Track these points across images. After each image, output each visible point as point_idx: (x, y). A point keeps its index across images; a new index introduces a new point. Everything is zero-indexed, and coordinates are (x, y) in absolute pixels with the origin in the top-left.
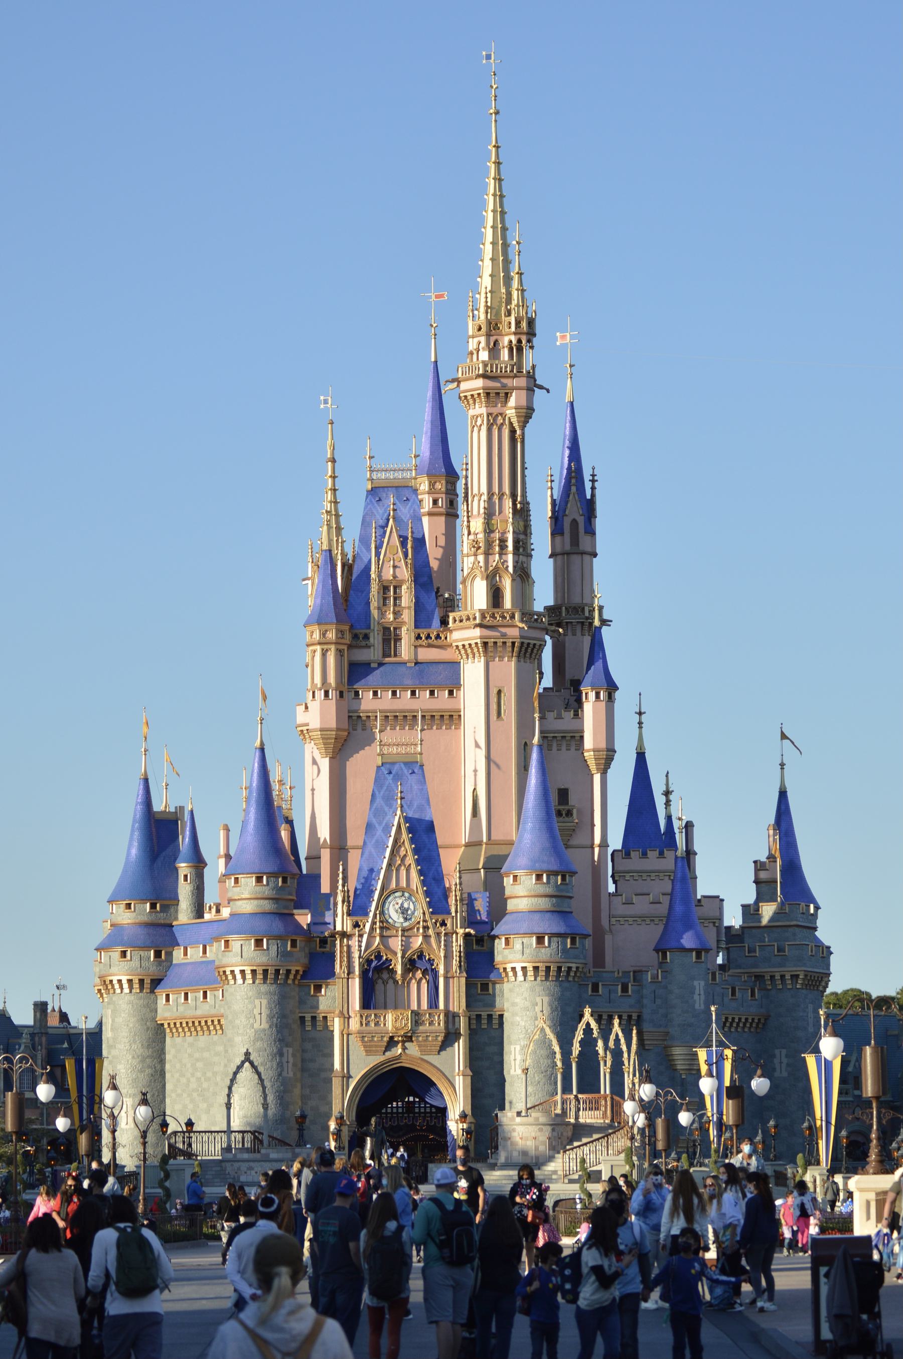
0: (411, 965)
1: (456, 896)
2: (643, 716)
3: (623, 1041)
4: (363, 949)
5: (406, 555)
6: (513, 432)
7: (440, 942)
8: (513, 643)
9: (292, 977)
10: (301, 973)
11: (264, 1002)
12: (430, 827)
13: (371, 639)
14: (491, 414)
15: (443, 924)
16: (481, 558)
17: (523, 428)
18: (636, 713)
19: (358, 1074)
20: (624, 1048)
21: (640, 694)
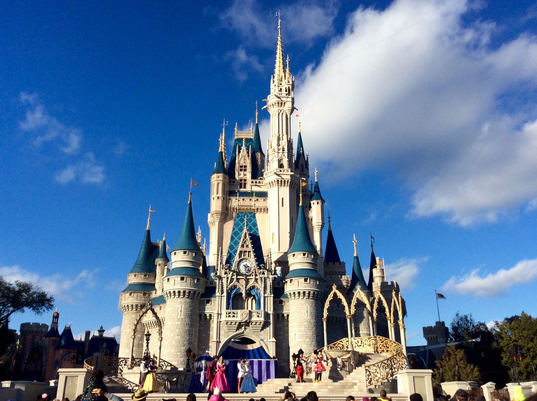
0: (249, 295)
1: (269, 262)
2: (330, 219)
3: (384, 302)
4: (228, 283)
5: (248, 156)
6: (287, 116)
7: (262, 281)
8: (288, 181)
9: (196, 295)
10: (201, 294)
11: (183, 306)
12: (258, 238)
13: (235, 182)
14: (279, 110)
15: (263, 273)
16: (276, 154)
17: (291, 114)
18: (328, 217)
19: (224, 340)
20: (386, 305)
21: (329, 211)
